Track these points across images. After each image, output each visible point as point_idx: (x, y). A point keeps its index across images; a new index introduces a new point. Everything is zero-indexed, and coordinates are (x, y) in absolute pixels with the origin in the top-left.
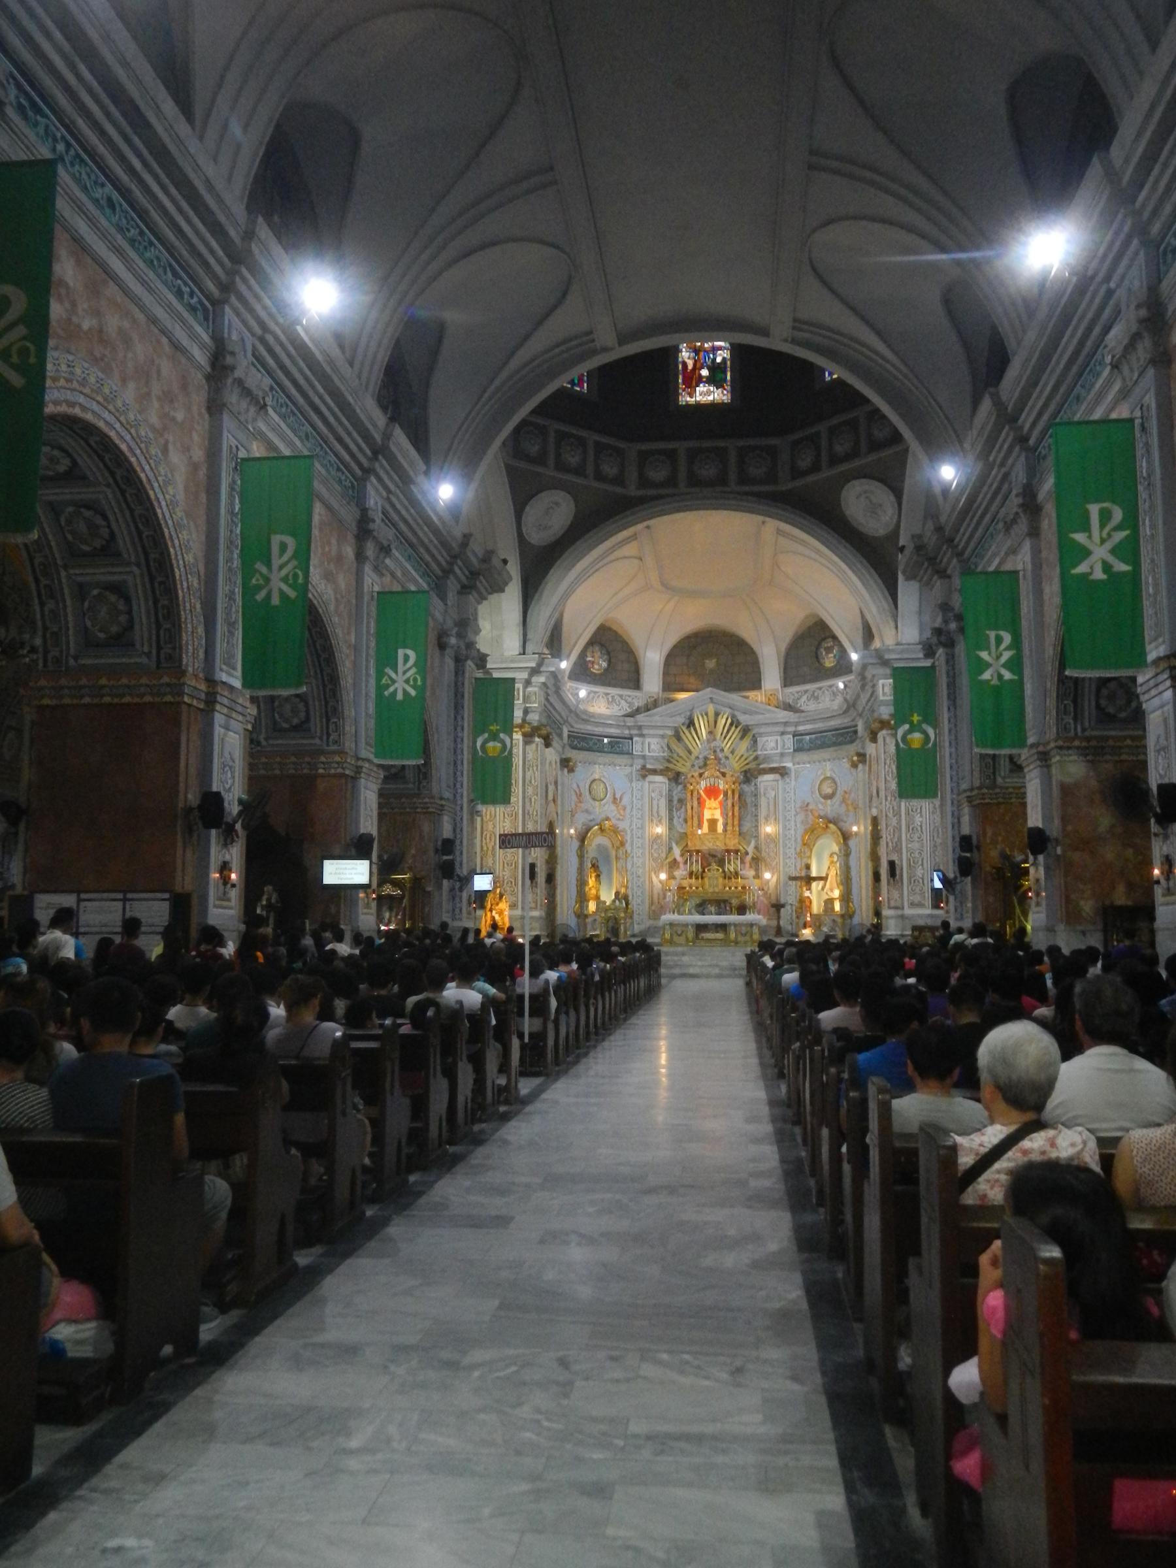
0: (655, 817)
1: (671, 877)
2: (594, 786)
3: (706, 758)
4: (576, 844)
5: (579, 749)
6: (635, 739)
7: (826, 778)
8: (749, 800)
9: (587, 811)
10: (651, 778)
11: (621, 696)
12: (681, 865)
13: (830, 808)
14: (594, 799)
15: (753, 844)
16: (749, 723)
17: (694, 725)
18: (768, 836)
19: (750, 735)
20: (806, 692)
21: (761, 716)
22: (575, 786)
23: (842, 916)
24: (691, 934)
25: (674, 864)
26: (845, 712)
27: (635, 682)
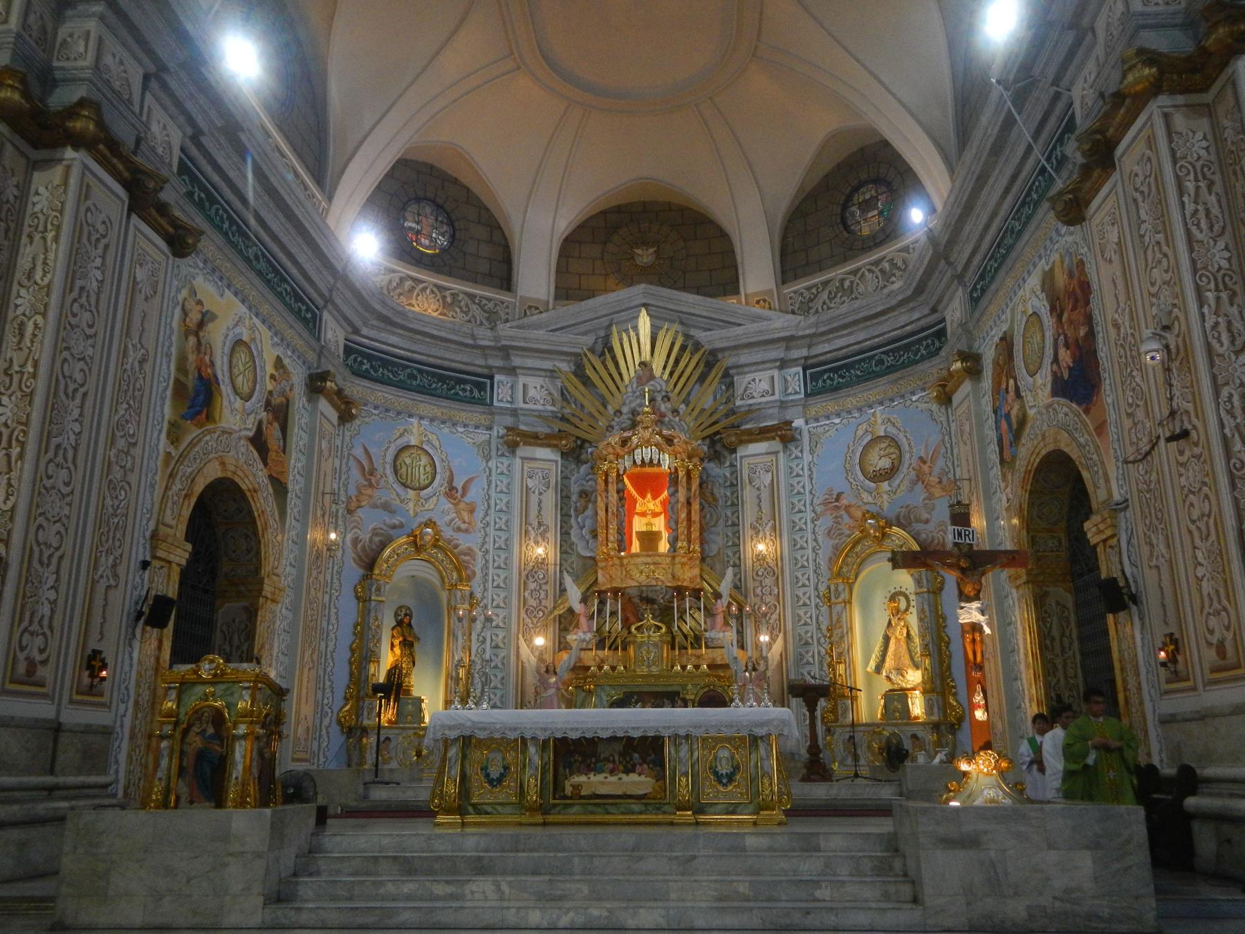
0: (532, 528)
1: (562, 646)
3: (634, 413)
4: (353, 572)
6: (497, 378)
7: (876, 440)
8: (720, 492)
9: (386, 507)
11: (472, 297)
12: (583, 620)
13: (886, 497)
14: (405, 485)
15: (730, 572)
16: (719, 345)
17: (611, 350)
18: (760, 558)
19: (716, 374)
20: (825, 284)
21: (739, 330)
22: (358, 452)
23: (936, 727)
25: (567, 621)
26: (920, 290)
27: (506, 282)
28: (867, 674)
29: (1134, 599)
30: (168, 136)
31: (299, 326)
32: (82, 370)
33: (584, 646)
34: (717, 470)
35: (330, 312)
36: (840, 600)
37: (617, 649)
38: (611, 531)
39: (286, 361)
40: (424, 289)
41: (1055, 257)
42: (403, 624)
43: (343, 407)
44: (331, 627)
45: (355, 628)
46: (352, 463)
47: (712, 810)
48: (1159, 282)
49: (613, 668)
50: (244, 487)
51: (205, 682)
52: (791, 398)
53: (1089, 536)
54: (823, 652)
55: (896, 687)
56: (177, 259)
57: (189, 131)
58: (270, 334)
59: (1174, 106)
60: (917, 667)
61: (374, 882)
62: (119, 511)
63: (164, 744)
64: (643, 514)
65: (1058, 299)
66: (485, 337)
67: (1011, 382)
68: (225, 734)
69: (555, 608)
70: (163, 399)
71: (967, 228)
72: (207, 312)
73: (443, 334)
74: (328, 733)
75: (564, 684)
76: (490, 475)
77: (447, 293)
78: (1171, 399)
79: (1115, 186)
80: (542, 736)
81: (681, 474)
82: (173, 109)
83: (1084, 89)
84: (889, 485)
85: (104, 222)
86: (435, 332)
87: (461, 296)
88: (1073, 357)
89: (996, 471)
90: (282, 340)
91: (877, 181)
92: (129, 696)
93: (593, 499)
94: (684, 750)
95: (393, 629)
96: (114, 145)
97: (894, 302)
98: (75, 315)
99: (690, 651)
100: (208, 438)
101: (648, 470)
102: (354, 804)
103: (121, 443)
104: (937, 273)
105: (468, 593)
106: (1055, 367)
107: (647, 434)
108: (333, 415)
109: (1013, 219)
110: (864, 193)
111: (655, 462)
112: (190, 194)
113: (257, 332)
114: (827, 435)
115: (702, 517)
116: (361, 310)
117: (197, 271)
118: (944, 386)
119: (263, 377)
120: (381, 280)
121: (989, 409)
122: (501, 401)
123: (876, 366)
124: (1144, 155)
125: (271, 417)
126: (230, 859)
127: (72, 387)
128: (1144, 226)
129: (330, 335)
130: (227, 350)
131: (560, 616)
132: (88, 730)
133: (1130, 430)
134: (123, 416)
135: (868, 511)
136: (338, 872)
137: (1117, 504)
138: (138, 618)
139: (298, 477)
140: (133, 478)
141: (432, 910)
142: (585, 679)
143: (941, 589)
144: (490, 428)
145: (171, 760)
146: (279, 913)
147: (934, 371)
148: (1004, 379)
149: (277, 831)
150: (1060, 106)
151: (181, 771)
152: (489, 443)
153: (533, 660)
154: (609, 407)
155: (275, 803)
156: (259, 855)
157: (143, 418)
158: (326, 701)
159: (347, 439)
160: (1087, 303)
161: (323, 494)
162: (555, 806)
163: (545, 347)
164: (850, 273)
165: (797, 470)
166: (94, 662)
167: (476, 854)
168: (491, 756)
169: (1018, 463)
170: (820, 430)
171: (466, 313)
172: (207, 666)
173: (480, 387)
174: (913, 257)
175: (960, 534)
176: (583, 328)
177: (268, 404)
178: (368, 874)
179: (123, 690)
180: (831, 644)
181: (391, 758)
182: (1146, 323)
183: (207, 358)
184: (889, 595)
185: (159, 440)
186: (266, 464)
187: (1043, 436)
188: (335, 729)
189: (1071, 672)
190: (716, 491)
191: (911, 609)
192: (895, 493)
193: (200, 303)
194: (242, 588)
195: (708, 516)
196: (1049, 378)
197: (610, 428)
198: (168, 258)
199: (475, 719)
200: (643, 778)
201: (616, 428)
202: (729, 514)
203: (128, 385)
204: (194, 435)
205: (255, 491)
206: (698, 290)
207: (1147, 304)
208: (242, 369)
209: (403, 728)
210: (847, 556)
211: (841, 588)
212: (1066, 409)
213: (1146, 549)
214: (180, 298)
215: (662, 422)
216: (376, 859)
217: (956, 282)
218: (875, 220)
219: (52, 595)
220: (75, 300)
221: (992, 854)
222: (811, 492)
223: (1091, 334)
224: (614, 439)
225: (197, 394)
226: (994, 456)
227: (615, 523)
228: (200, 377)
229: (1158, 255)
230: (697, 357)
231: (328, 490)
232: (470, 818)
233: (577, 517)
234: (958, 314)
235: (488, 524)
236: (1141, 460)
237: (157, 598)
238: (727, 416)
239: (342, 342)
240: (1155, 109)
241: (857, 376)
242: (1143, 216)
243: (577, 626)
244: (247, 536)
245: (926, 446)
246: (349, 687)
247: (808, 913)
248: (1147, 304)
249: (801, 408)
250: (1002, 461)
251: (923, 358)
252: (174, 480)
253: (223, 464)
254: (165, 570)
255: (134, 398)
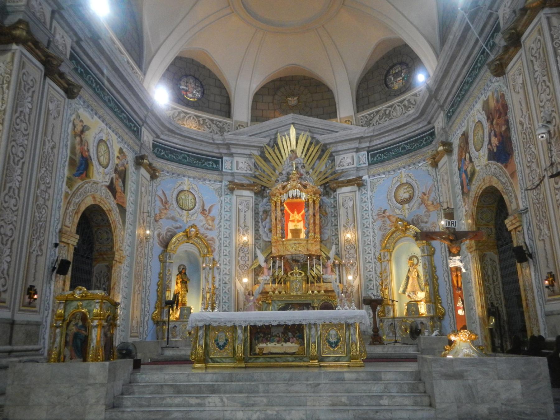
0: (241, 228)
1: (256, 282)
2: (182, 196)
3: (288, 174)
4: (158, 249)
5: (167, 160)
6: (224, 158)
7: (402, 184)
8: (329, 210)
9: (173, 219)
10: (237, 192)
11: (212, 121)
13: (407, 211)
14: (182, 209)
15: (334, 247)
17: (277, 145)
18: (348, 241)
19: (326, 155)
20: (377, 112)
21: (337, 134)
22: (160, 193)
23: (432, 318)
24: (240, 348)
25: (258, 271)
26: (422, 114)
27: (228, 114)
28: (399, 294)
29: (531, 256)
30: (64, 41)
31: (131, 134)
32: (22, 151)
33: (266, 282)
34: (327, 200)
35: (146, 128)
36: (386, 259)
37: (281, 283)
38: (278, 229)
39: (124, 150)
40: (190, 117)
41: (489, 93)
42: (182, 273)
43: (152, 172)
44: (148, 275)
45: (159, 275)
46: (157, 198)
47: (327, 360)
48: (545, 100)
49: (280, 292)
50: (105, 209)
51: (78, 300)
52: (362, 166)
53: (507, 226)
54: (378, 284)
55: (413, 300)
56: (70, 100)
57: (75, 39)
58: (116, 137)
59: (552, 14)
60: (422, 290)
61: (161, 398)
62: (42, 219)
63: (58, 330)
64: (293, 221)
65: (491, 113)
66: (218, 139)
67: (467, 155)
68: (87, 325)
69: (252, 265)
70: (64, 167)
71: (446, 83)
72: (85, 126)
73: (199, 138)
74: (147, 324)
75: (257, 300)
76: (222, 203)
77: (201, 119)
78: (551, 157)
79: (521, 56)
80: (244, 325)
81: (311, 202)
82: (67, 28)
83: (504, 10)
84: (409, 206)
85: (32, 80)
86: (195, 137)
87: (207, 121)
88: (499, 141)
89: (460, 197)
90: (122, 140)
91: (401, 63)
92: (49, 307)
93: (269, 214)
94: (313, 331)
95: (177, 275)
96: (36, 43)
97: (410, 120)
98: (18, 125)
99: (316, 284)
100: (86, 185)
101: (295, 200)
102: (156, 357)
103: (43, 187)
104: (431, 105)
105: (212, 259)
106: (489, 146)
107: (294, 183)
108: (148, 176)
109: (468, 76)
110: (395, 69)
111: (298, 196)
112: (76, 69)
113: (110, 137)
114: (379, 183)
115: (321, 222)
116: (160, 127)
117: (80, 106)
118: (434, 159)
119: (113, 157)
120: (169, 113)
121: (456, 168)
122: (226, 169)
123: (402, 150)
124: (536, 39)
125: (117, 176)
126: (89, 387)
127: (17, 159)
128: (536, 74)
129: (145, 138)
130: (95, 144)
131: (255, 268)
132: (28, 324)
133: (529, 174)
134: (43, 174)
135: (399, 218)
136: (144, 393)
137: (522, 211)
138: (53, 270)
139: (131, 204)
140: (49, 203)
141: (188, 412)
142: (267, 297)
143: (433, 254)
144: (221, 182)
145: (61, 338)
146: (113, 413)
147: (430, 152)
148: (464, 154)
149: (112, 374)
150: (492, 20)
151: (66, 343)
152: (221, 188)
153: (242, 289)
154: (277, 171)
155: (113, 359)
156: (102, 385)
157: (54, 175)
158: (146, 309)
159: (154, 187)
160: (506, 114)
161: (143, 213)
162: (251, 358)
163: (246, 143)
164: (388, 107)
165: (365, 199)
166: (31, 291)
167: (211, 383)
168: (219, 334)
169: (471, 193)
170: (375, 181)
171: (210, 128)
172: (78, 292)
173: (216, 162)
174: (419, 99)
175: (449, 223)
176: (264, 134)
177: (116, 171)
178: (158, 393)
179: (46, 305)
180: (382, 280)
181: (177, 335)
182: (538, 121)
183: (86, 148)
184: (408, 257)
185: (62, 186)
186: (115, 198)
187: (484, 180)
188: (151, 322)
189: (497, 292)
190: (327, 210)
191: (419, 264)
192: (411, 209)
193: (81, 121)
194: (105, 256)
195: (323, 221)
196: (487, 152)
197: (277, 181)
198: (65, 99)
199: (211, 317)
200: (293, 344)
201: (280, 181)
202: (333, 220)
203: (46, 159)
204: (79, 184)
205: (110, 211)
206: (318, 116)
207: (538, 111)
208: (103, 153)
209: (183, 321)
210: (389, 239)
211: (386, 254)
212: (495, 166)
213: (537, 232)
214: (72, 118)
215: (302, 178)
216: (162, 386)
217: (440, 109)
218: (401, 82)
219: (8, 259)
220: (18, 117)
221: (470, 382)
222: (371, 210)
223: (508, 129)
224: (279, 186)
225: (81, 164)
226: (460, 192)
227: (280, 225)
228: (82, 157)
229: (544, 87)
230: (317, 147)
231: (145, 211)
232: (209, 365)
233: (262, 222)
234: (441, 124)
235: (221, 226)
236: (534, 189)
237: (62, 261)
238: (332, 174)
239: (151, 142)
240: (542, 15)
241: (393, 155)
242: (536, 68)
243: (263, 273)
244: (107, 232)
245: (426, 189)
246: (157, 303)
247: (377, 412)
248: (538, 111)
249: (366, 170)
250: (463, 193)
251: (424, 146)
252: (70, 205)
253: (94, 198)
254: (66, 247)
255: (49, 166)
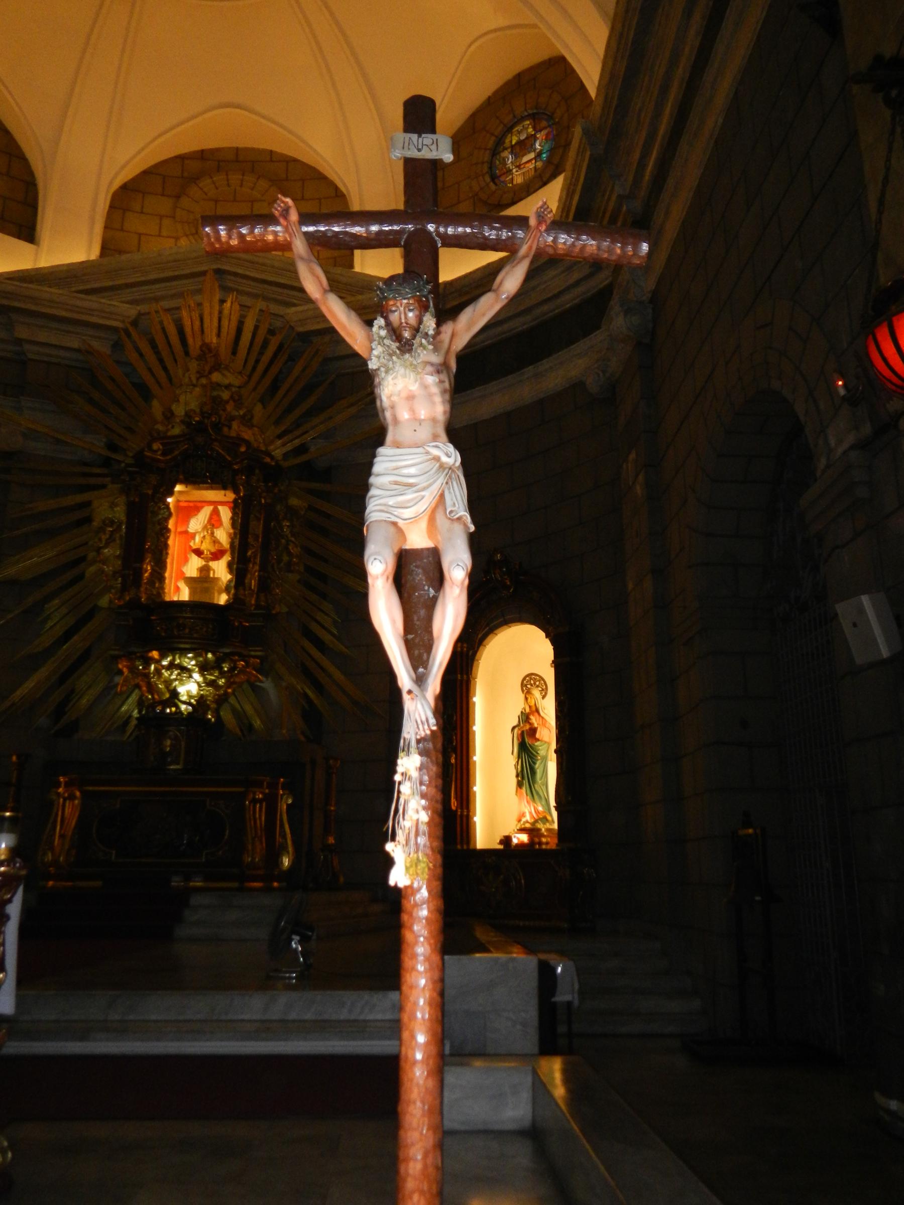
110: (519, 132)
154: (155, 403)
163: (64, 314)
218: (531, 166)
